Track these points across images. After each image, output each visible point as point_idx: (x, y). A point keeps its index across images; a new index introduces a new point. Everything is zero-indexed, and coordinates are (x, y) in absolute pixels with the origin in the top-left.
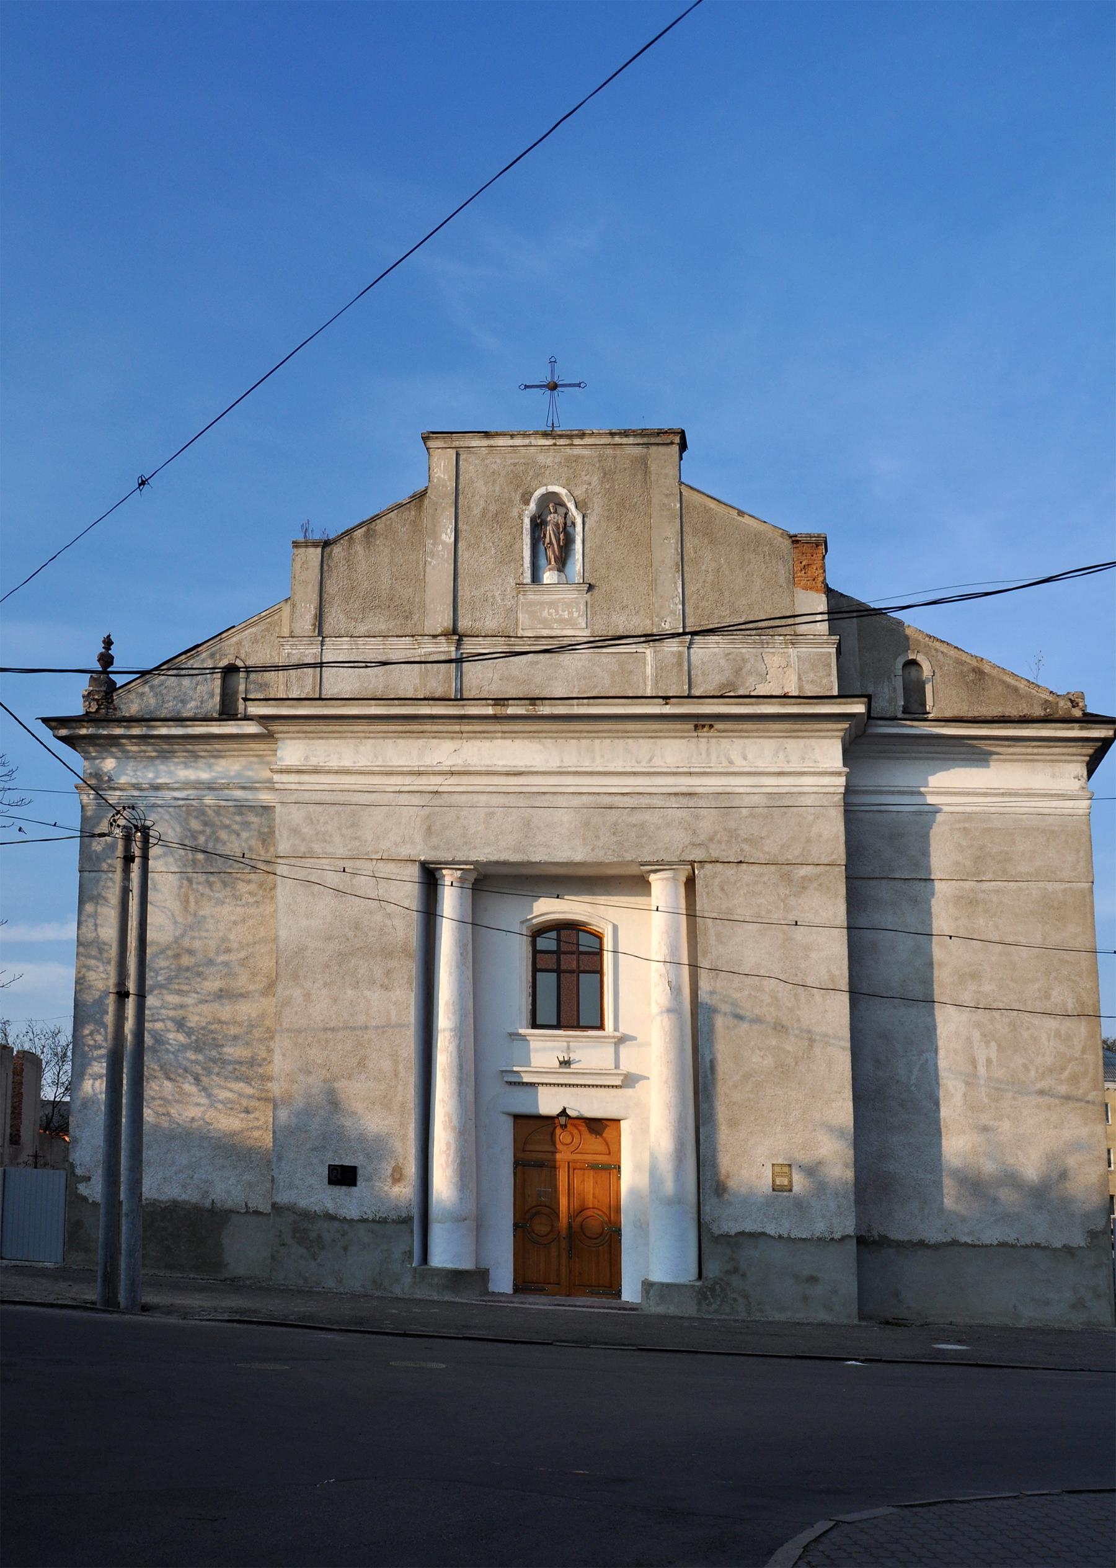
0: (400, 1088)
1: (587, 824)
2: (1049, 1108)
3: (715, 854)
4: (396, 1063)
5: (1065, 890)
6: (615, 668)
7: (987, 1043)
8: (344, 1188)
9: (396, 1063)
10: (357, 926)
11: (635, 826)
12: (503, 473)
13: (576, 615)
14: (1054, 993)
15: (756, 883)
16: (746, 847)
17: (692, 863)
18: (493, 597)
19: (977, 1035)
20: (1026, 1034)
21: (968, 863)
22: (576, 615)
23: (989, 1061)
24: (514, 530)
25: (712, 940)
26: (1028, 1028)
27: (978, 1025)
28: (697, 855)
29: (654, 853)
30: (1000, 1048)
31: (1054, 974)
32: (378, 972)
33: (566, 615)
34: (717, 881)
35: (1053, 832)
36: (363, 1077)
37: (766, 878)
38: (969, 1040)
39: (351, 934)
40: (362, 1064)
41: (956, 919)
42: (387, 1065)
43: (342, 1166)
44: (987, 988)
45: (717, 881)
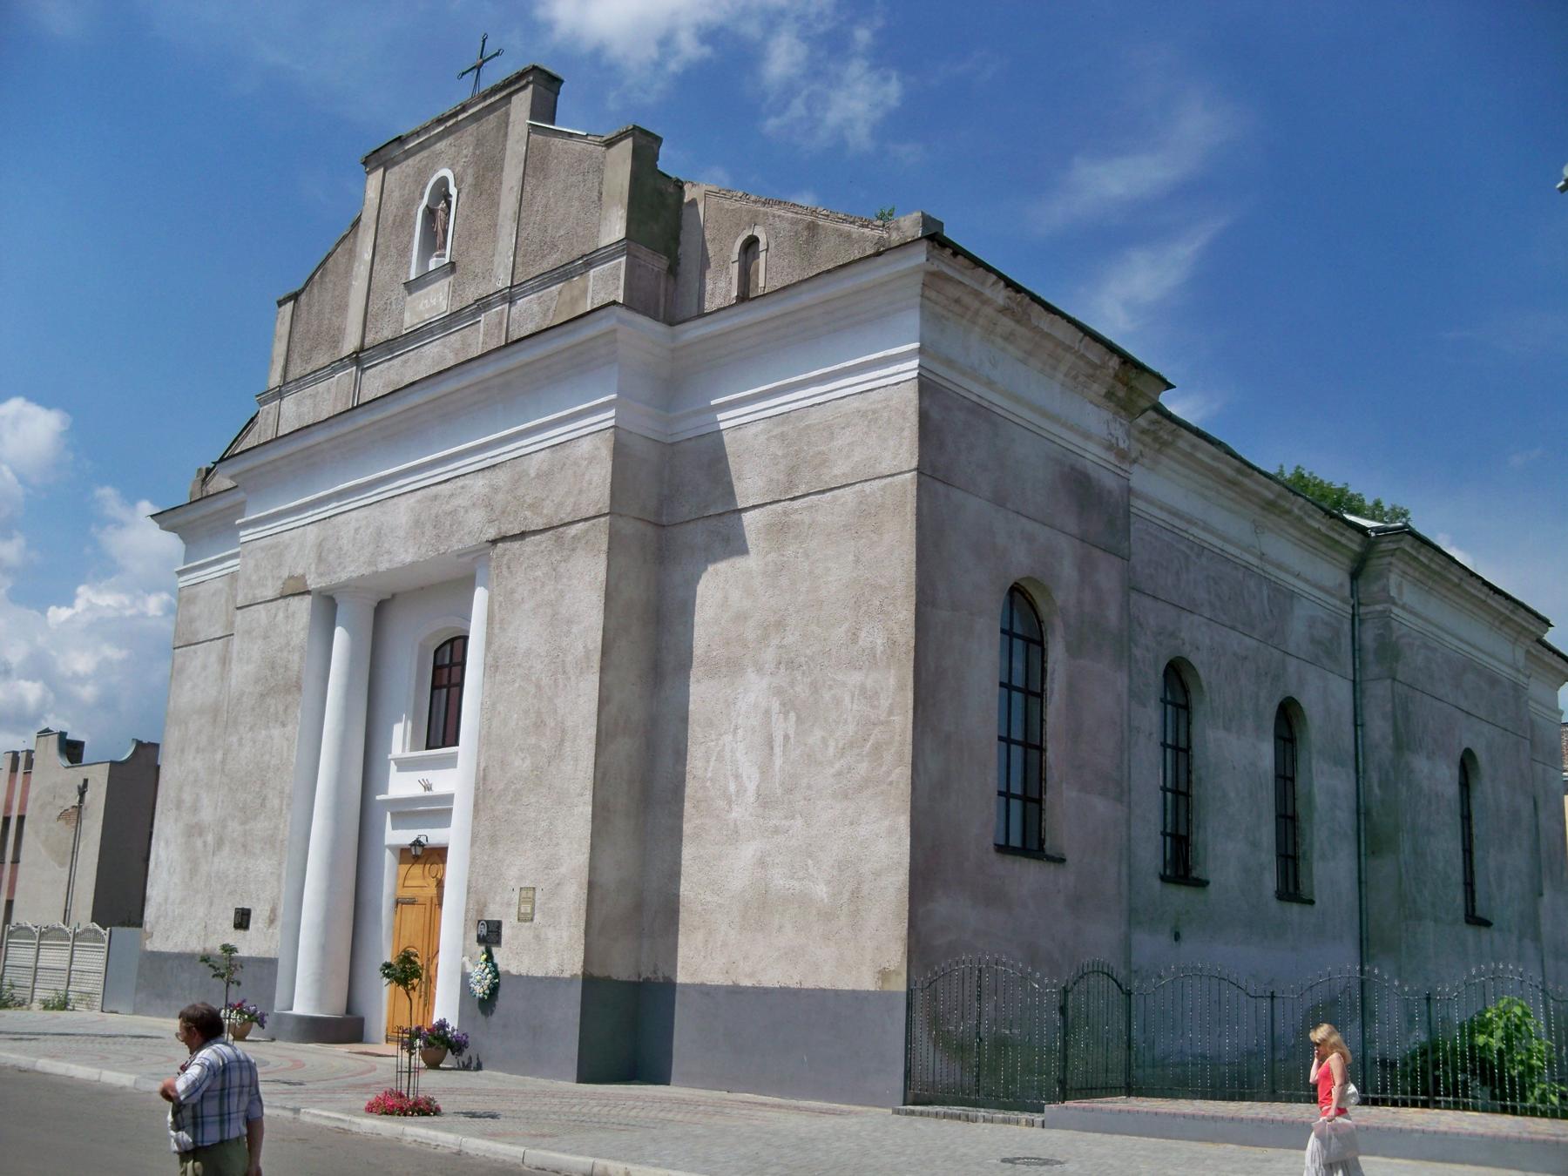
2: (846, 796)
5: (884, 489)
7: (786, 714)
14: (863, 634)
19: (776, 706)
20: (827, 696)
21: (781, 477)
23: (786, 737)
26: (831, 687)
27: (779, 691)
30: (799, 720)
31: (864, 608)
35: (874, 412)
38: (767, 712)
41: (768, 553)
44: (790, 639)
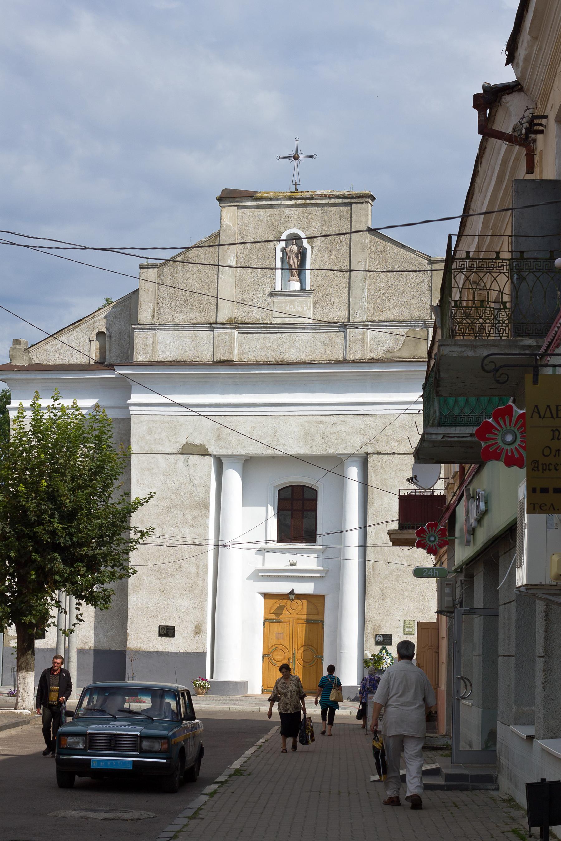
0: (200, 582)
1: (307, 433)
3: (380, 449)
4: (198, 567)
6: (327, 341)
8: (168, 638)
9: (198, 567)
10: (177, 492)
11: (335, 433)
12: (265, 221)
13: (305, 309)
15: (402, 464)
16: (396, 444)
17: (367, 454)
18: (258, 298)
22: (305, 309)
24: (270, 257)
25: (375, 496)
28: (370, 450)
29: (344, 449)
32: (189, 518)
33: (299, 309)
34: (379, 464)
36: (179, 576)
37: (406, 462)
39: (173, 497)
40: (179, 569)
42: (193, 569)
43: (167, 626)
45: (379, 464)
